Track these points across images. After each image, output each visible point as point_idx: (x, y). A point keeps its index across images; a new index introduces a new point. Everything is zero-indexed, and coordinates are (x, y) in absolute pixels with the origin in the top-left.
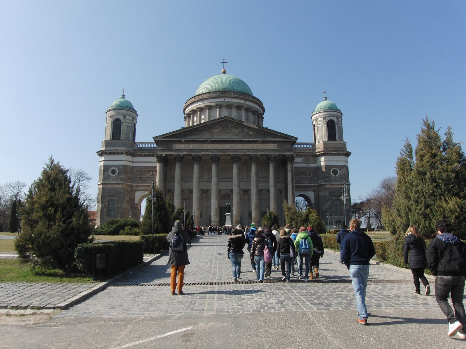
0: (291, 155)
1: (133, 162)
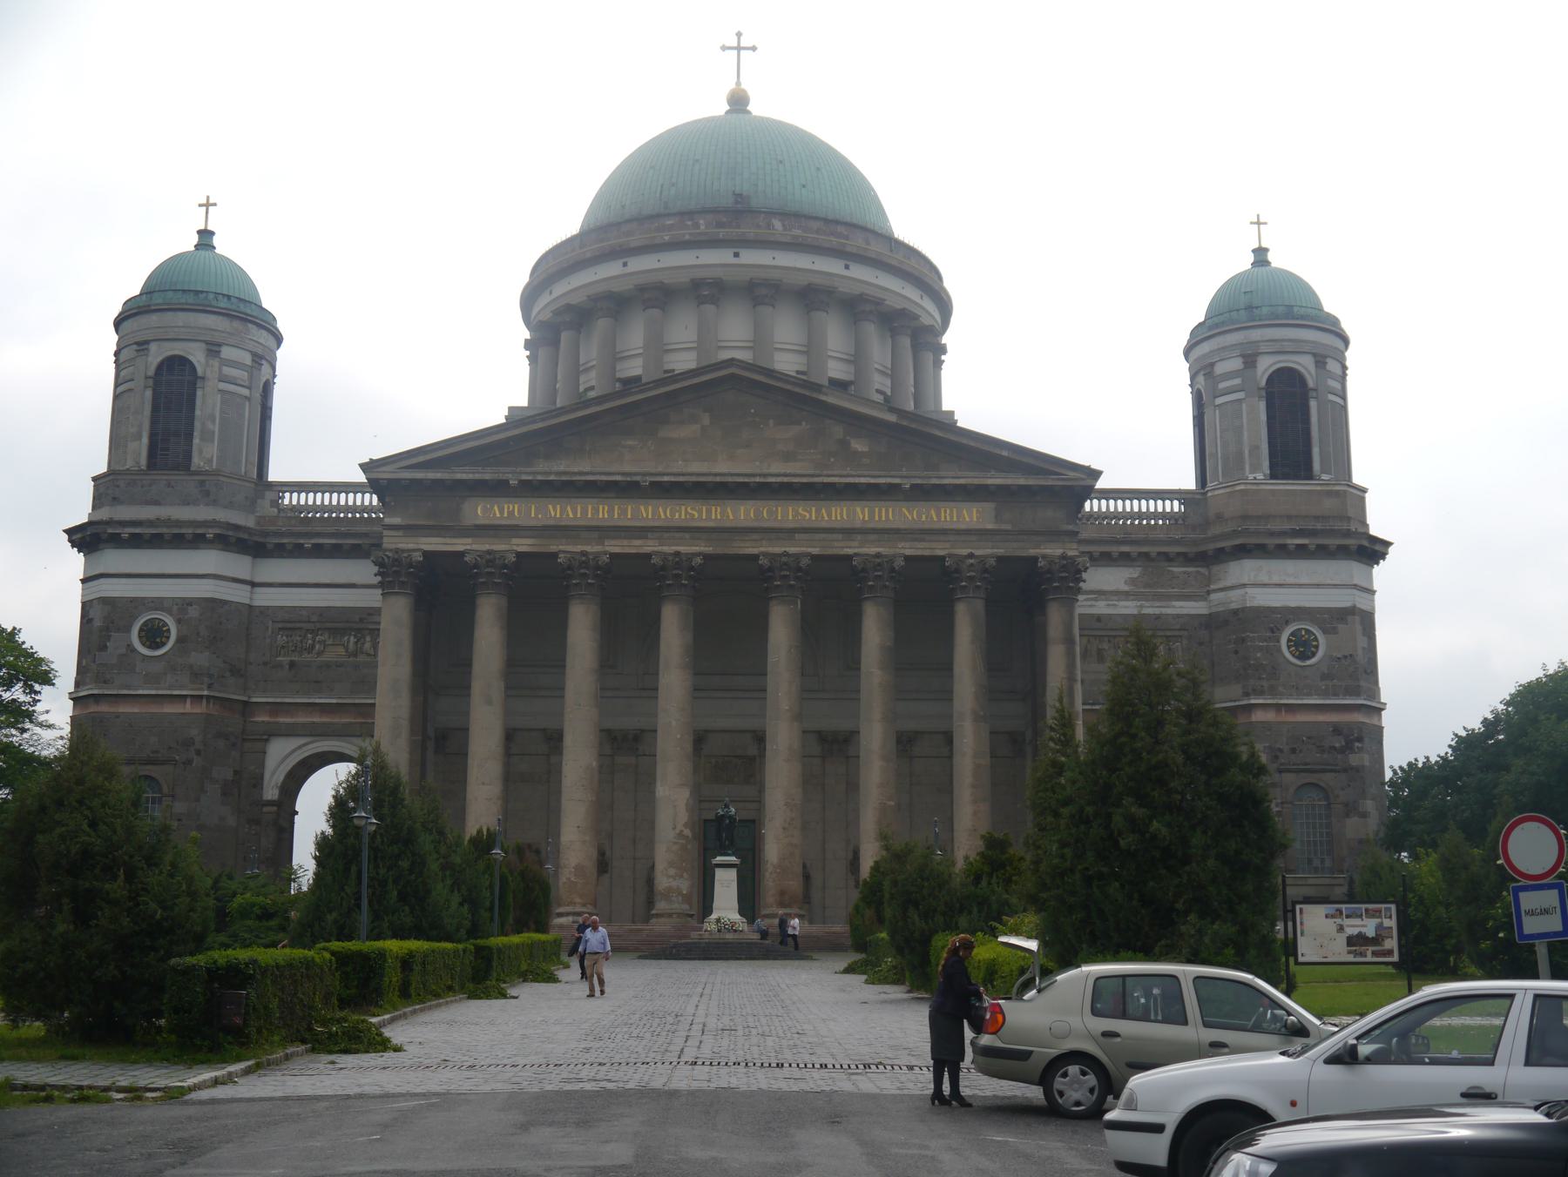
0: (1064, 557)
1: (253, 584)
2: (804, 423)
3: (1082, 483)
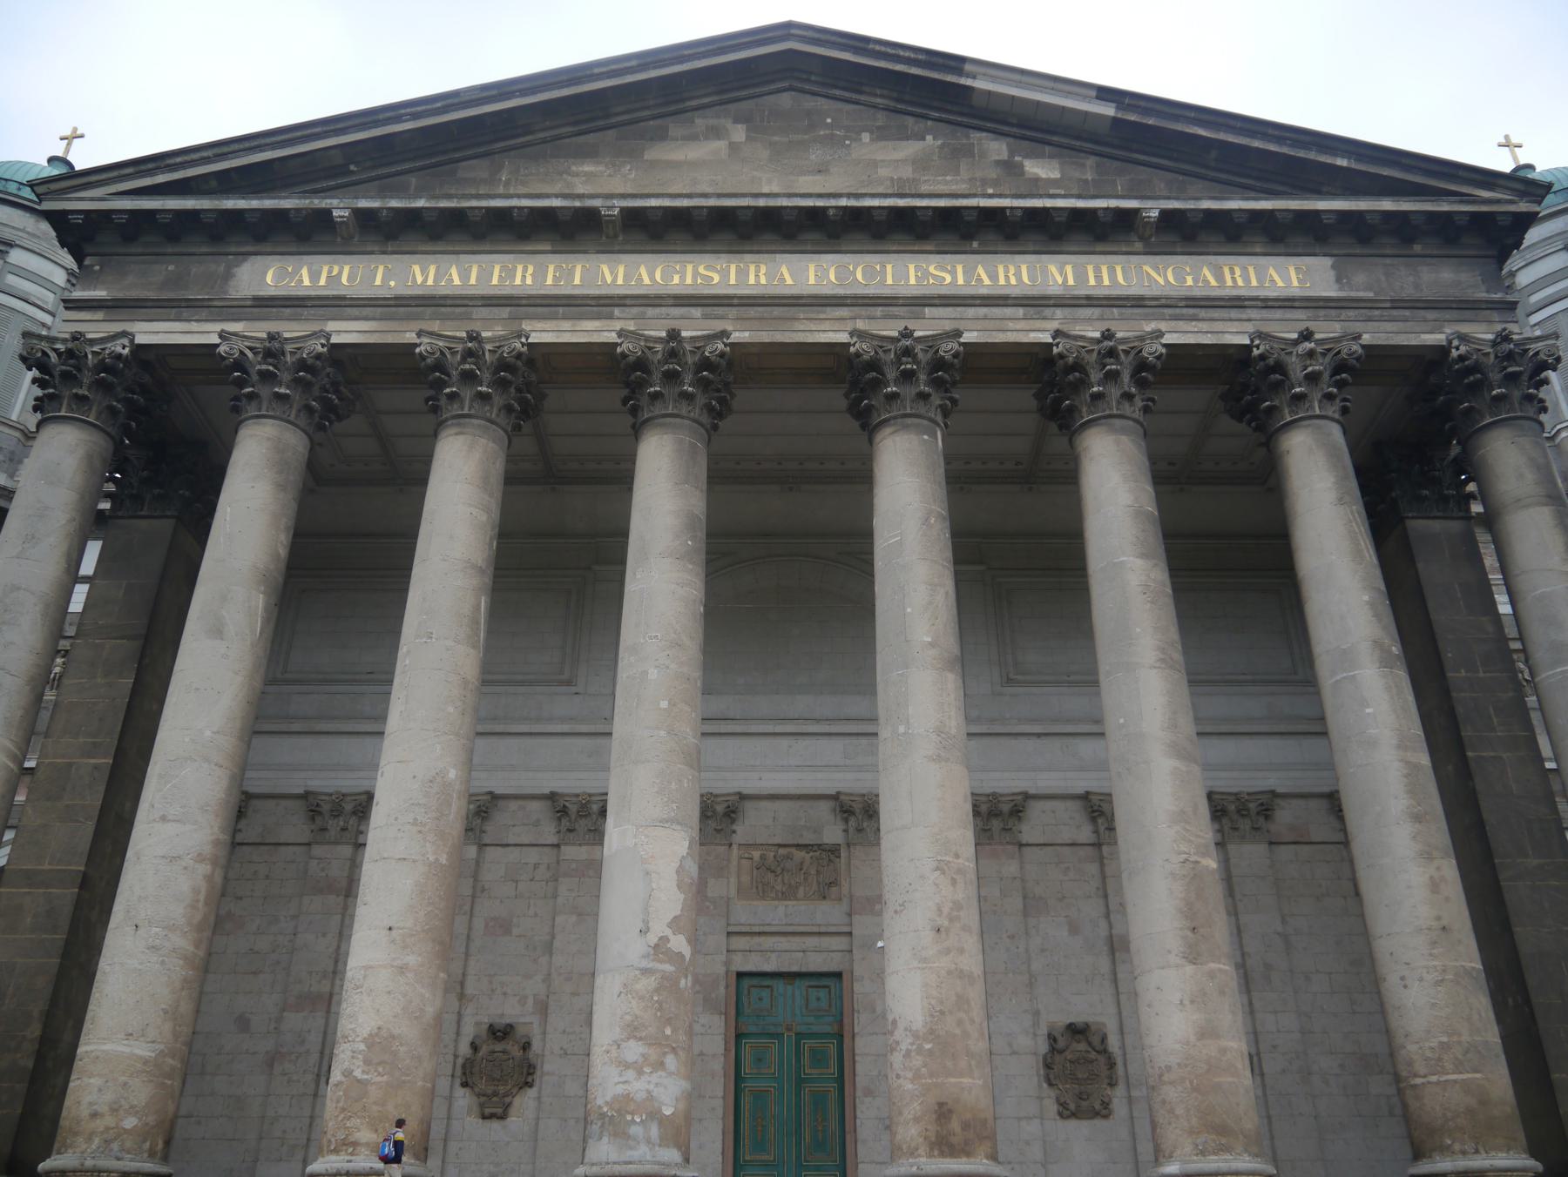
2: (929, 138)
3: (1512, 208)
